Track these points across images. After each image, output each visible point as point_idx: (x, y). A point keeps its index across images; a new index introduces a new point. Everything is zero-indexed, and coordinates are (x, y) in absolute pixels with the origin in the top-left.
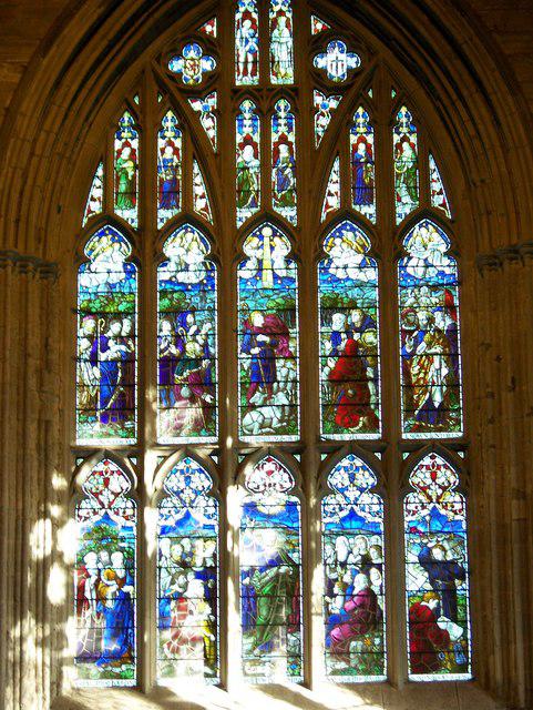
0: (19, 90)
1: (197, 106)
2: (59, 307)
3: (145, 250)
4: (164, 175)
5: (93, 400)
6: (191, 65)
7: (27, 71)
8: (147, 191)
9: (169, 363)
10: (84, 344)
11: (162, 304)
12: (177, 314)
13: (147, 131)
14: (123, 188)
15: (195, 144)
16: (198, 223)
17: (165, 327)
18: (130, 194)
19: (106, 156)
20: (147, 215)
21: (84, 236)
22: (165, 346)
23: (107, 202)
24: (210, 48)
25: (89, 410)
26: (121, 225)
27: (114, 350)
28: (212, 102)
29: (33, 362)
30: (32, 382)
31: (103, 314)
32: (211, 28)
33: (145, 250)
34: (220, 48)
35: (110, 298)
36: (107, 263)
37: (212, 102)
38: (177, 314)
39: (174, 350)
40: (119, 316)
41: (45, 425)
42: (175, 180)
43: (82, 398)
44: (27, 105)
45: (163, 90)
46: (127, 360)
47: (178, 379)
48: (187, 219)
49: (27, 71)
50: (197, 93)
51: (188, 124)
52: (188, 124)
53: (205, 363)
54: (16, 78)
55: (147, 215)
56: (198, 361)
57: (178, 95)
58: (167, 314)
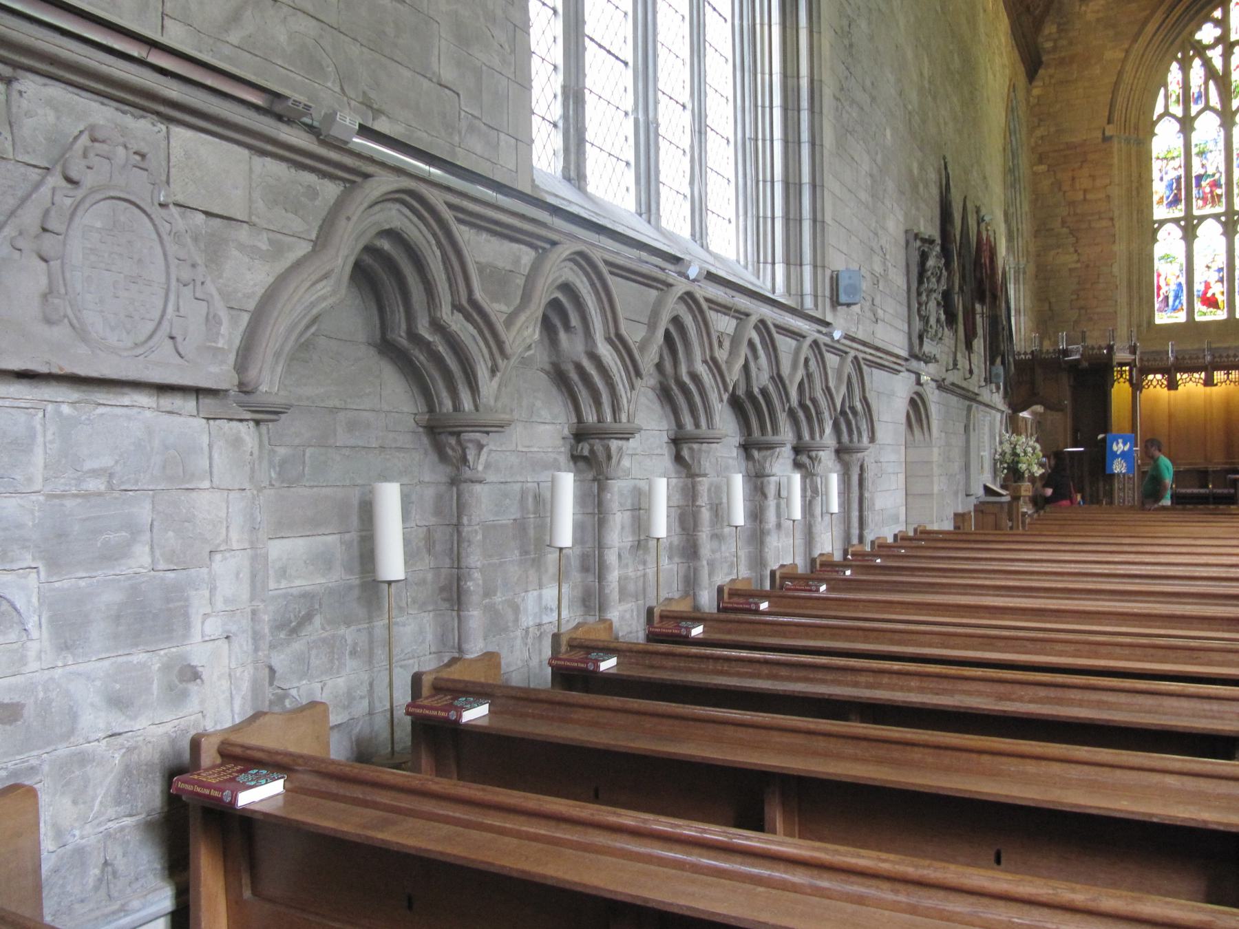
0: (1125, 60)
1: (1209, 53)
2: (1142, 160)
3: (1186, 124)
4: (1194, 90)
5: (1162, 198)
6: (1207, 33)
7: (1127, 51)
8: (1186, 99)
9: (1199, 178)
10: (1156, 175)
11: (1194, 150)
12: (1202, 154)
13: (1185, 67)
14: (1174, 98)
15: (1210, 72)
16: (1213, 110)
17: (1196, 162)
18: (1178, 101)
19: (1166, 86)
20: (1187, 109)
21: (1154, 124)
22: (1197, 170)
23: (1166, 106)
24: (1217, 23)
25: (1161, 201)
26: (1174, 116)
27: (1173, 174)
28: (1219, 49)
29: (1135, 185)
30: (1134, 193)
31: (1166, 158)
32: (1218, 14)
33: (1186, 124)
34: (1223, 23)
35: (1169, 152)
36: (1166, 138)
37: (1219, 49)
38: (1202, 154)
39: (1202, 171)
40: (1173, 158)
41: (1140, 212)
42: (1200, 92)
43: (1156, 198)
44: (1129, 67)
45: (1194, 48)
46: (1178, 179)
47: (1203, 184)
48: (1207, 107)
49: (1127, 51)
50: (1212, 47)
51: (1207, 63)
52: (1207, 63)
53: (1217, 176)
54: (1122, 55)
55: (1187, 109)
56: (1213, 175)
57: (1201, 49)
58: (1197, 154)
